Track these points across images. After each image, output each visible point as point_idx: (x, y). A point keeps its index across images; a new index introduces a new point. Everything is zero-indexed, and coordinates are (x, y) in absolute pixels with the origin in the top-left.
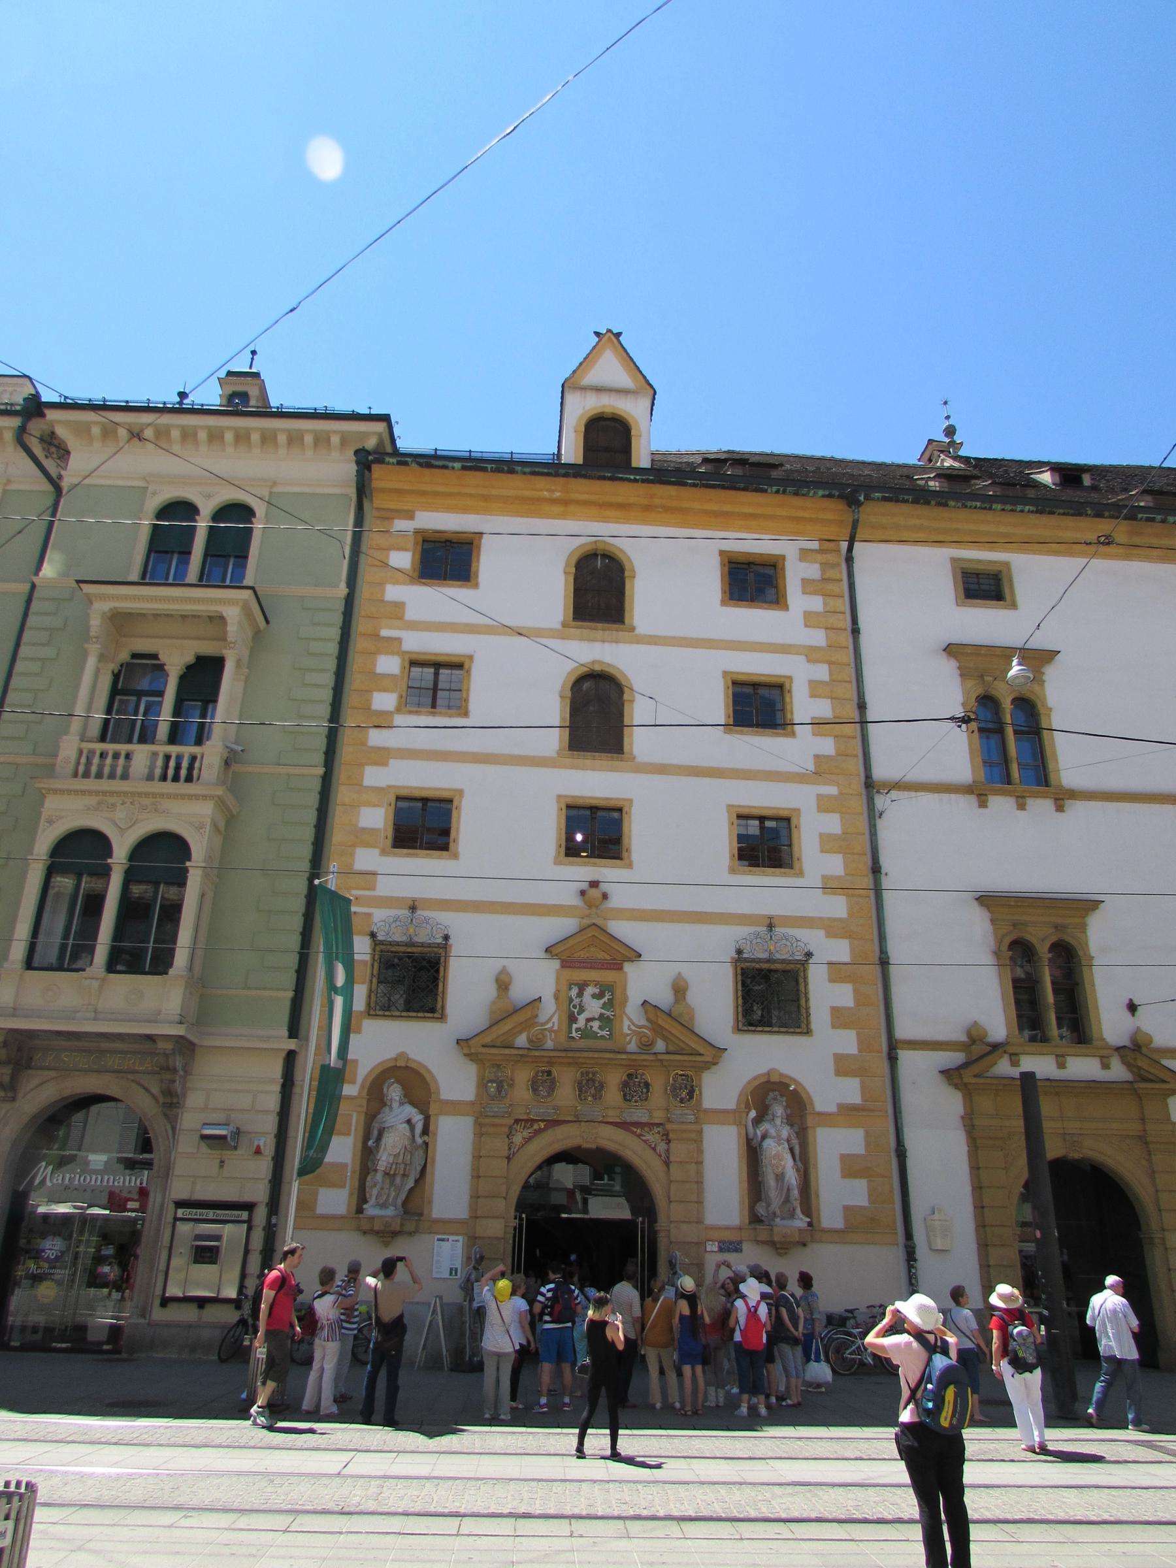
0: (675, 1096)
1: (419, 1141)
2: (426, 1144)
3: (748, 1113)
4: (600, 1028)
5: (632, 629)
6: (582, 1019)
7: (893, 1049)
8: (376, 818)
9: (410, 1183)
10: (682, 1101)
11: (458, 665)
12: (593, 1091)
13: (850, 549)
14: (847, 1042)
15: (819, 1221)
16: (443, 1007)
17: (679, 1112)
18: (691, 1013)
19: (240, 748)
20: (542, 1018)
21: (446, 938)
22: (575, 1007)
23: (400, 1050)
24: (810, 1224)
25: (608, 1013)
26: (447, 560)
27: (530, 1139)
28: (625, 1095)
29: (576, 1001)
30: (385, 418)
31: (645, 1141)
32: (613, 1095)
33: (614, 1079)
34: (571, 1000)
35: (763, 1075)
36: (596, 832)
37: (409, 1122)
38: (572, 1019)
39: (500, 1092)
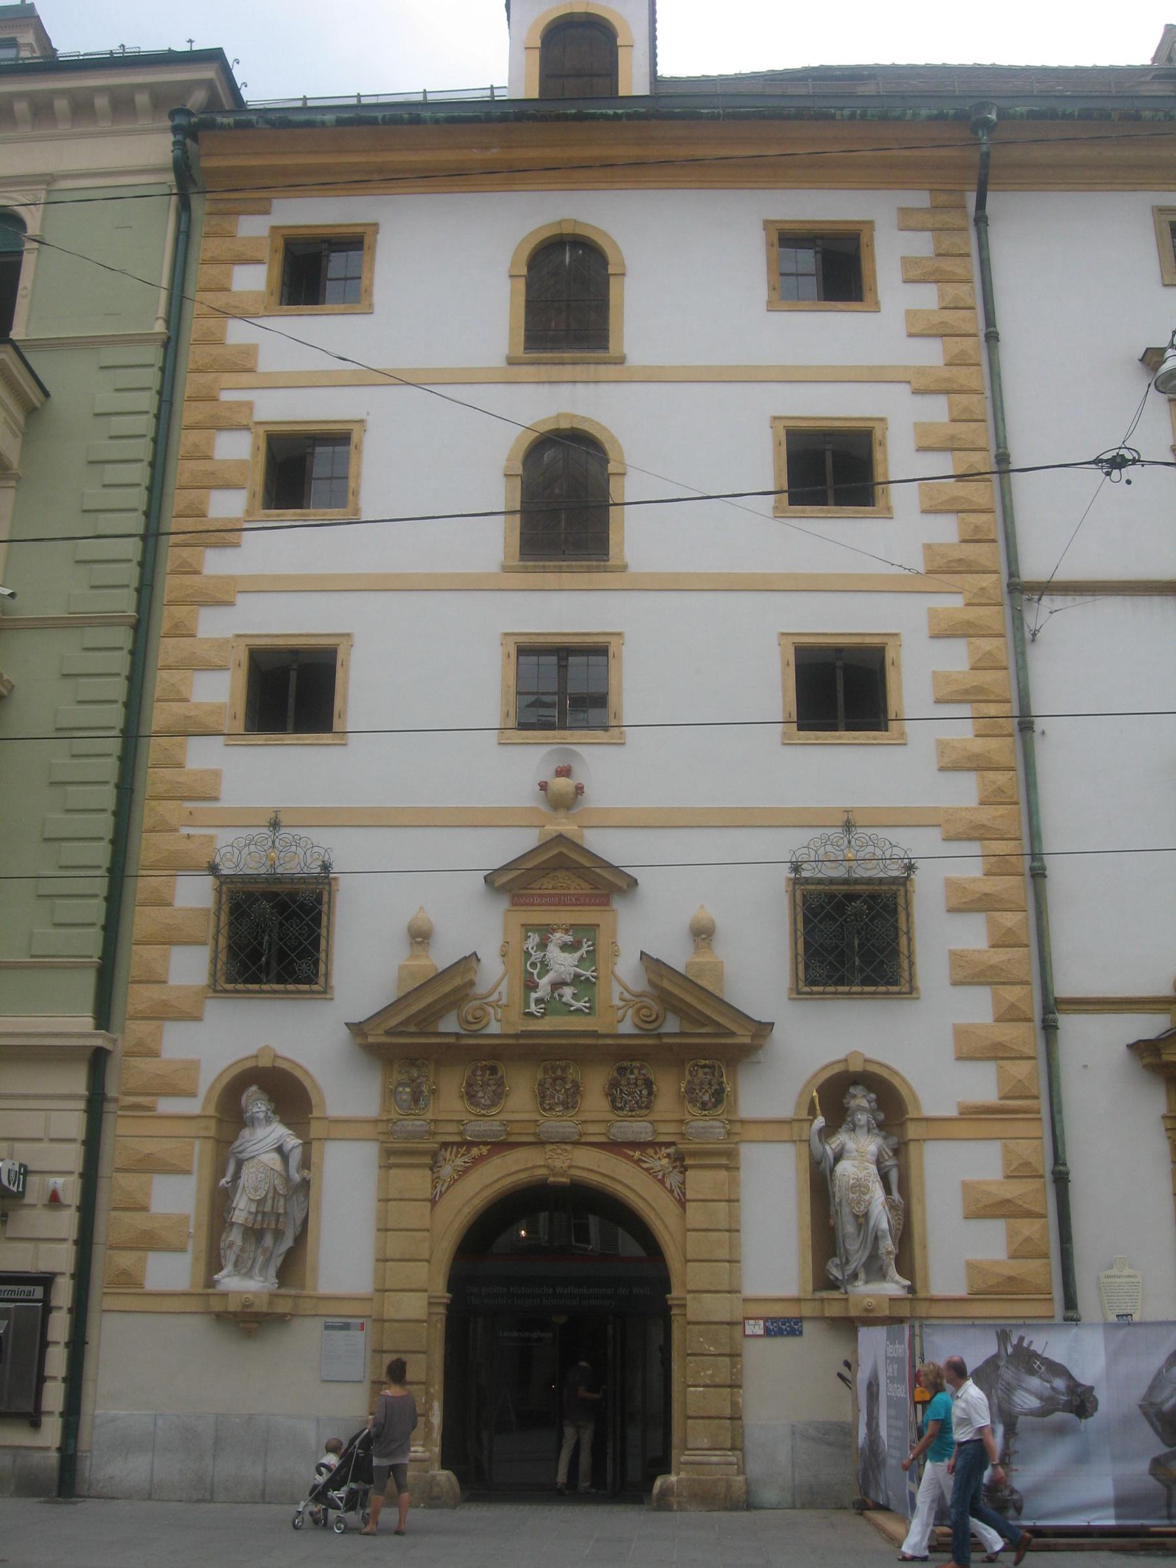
0: (692, 1101)
2: (306, 1184)
3: (812, 1121)
5: (620, 361)
6: (544, 982)
7: (1052, 1010)
8: (221, 690)
9: (288, 1243)
11: (339, 439)
13: (981, 204)
14: (977, 1008)
15: (926, 1286)
16: (327, 975)
18: (717, 970)
19: (7, 591)
20: (481, 988)
21: (326, 867)
22: (534, 965)
24: (911, 1289)
25: (588, 974)
26: (313, 273)
28: (613, 1101)
29: (536, 956)
30: (215, 56)
31: (647, 1170)
32: (595, 1102)
34: (528, 954)
35: (839, 1062)
36: (563, 689)
37: (279, 1150)
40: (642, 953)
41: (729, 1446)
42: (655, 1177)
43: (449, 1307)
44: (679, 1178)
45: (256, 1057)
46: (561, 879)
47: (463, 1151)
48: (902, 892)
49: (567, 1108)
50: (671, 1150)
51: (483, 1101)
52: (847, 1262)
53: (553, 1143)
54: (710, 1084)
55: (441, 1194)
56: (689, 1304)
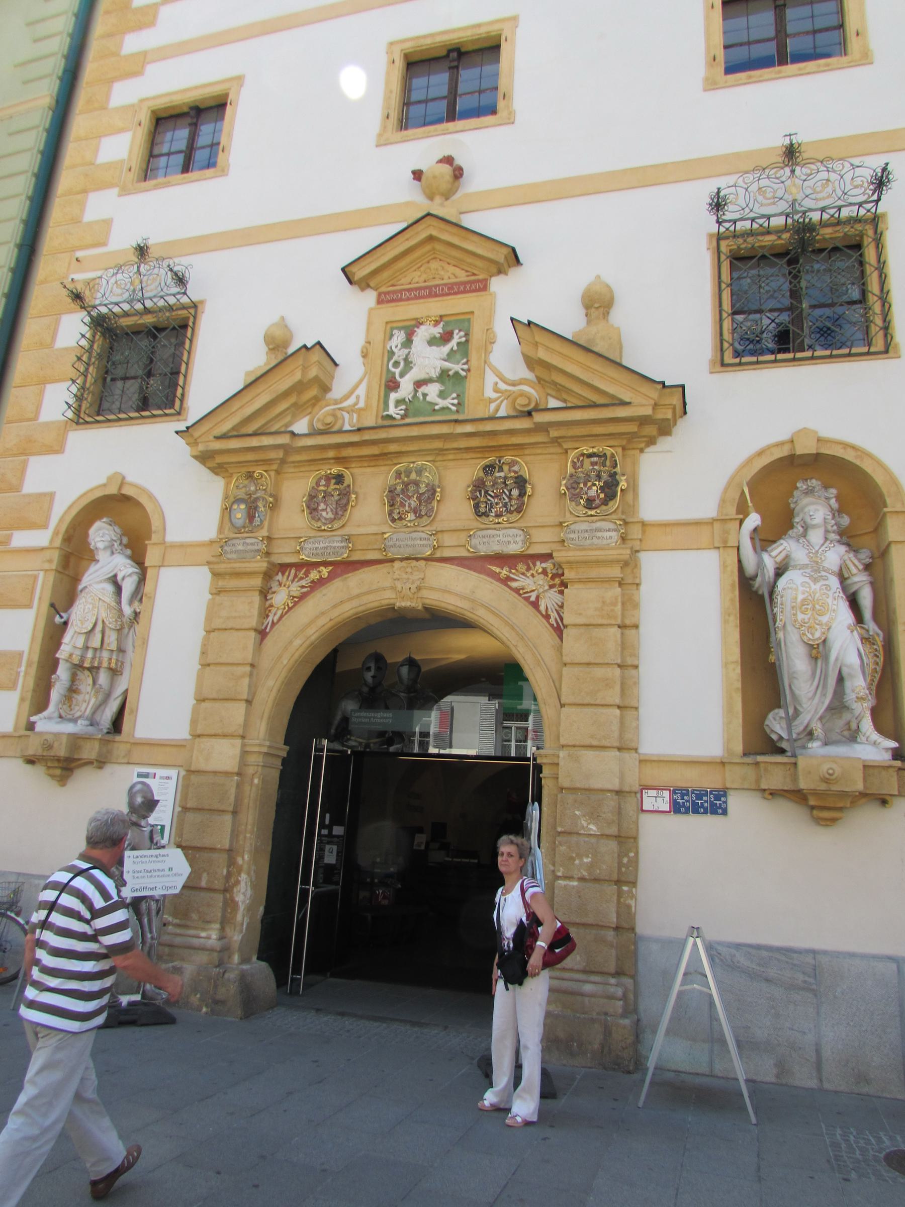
0: (575, 498)
1: (127, 610)
4: (442, 395)
10: (590, 504)
12: (414, 502)
17: (584, 526)
23: (111, 472)
27: (303, 597)
28: (476, 506)
29: (400, 354)
31: (517, 591)
32: (455, 508)
33: (458, 478)
34: (391, 353)
35: (781, 444)
38: (392, 385)
39: (251, 517)
40: (512, 319)
41: (612, 969)
42: (527, 599)
43: (284, 761)
44: (558, 598)
45: (105, 485)
46: (432, 260)
47: (301, 574)
48: (870, 233)
49: (421, 516)
50: (548, 565)
51: (324, 514)
52: (797, 713)
53: (402, 560)
54: (599, 477)
55: (273, 624)
56: (561, 763)
